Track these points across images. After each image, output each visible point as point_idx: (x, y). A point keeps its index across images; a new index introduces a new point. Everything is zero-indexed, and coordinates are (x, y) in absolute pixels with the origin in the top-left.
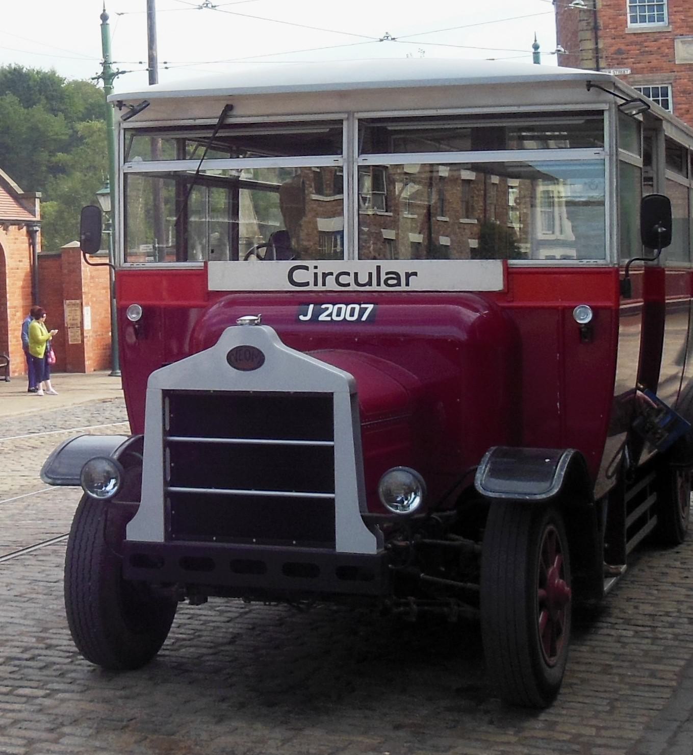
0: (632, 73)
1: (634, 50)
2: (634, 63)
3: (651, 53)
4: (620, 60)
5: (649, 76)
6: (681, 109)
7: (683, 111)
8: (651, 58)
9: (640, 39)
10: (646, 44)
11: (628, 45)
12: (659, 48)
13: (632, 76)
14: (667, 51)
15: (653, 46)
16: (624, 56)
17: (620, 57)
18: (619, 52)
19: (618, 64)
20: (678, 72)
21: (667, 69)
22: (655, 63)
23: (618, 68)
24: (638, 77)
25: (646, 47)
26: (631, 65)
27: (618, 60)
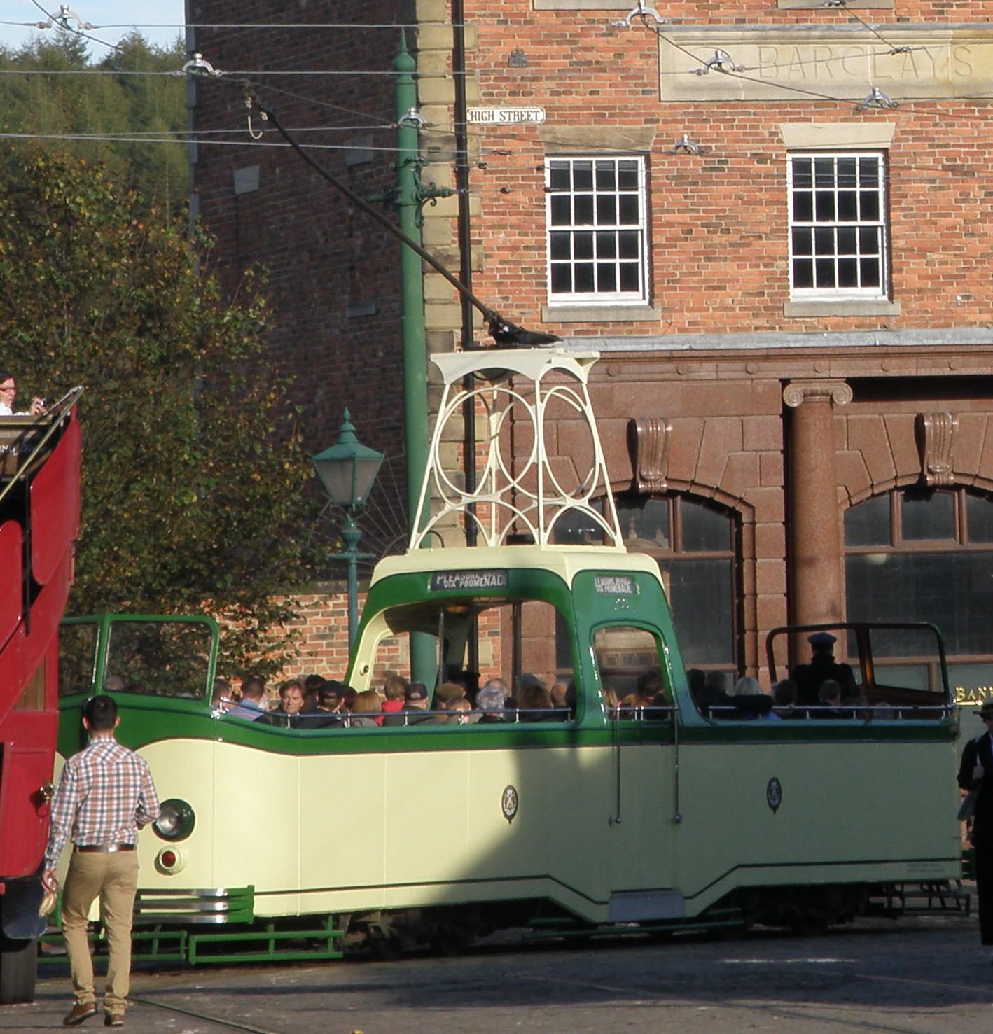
0: (547, 122)
1: (556, 57)
2: (554, 93)
3: (599, 67)
4: (518, 82)
5: (595, 129)
6: (671, 225)
7: (677, 230)
8: (594, 80)
9: (570, 30)
10: (585, 41)
11: (540, 43)
12: (619, 55)
13: (549, 127)
14: (638, 63)
15: (600, 48)
16: (529, 71)
17: (517, 73)
18: (516, 59)
19: (512, 93)
20: (665, 122)
21: (637, 115)
22: (607, 94)
23: (511, 105)
24: (562, 130)
25: (586, 49)
26: (548, 96)
27: (516, 77)
